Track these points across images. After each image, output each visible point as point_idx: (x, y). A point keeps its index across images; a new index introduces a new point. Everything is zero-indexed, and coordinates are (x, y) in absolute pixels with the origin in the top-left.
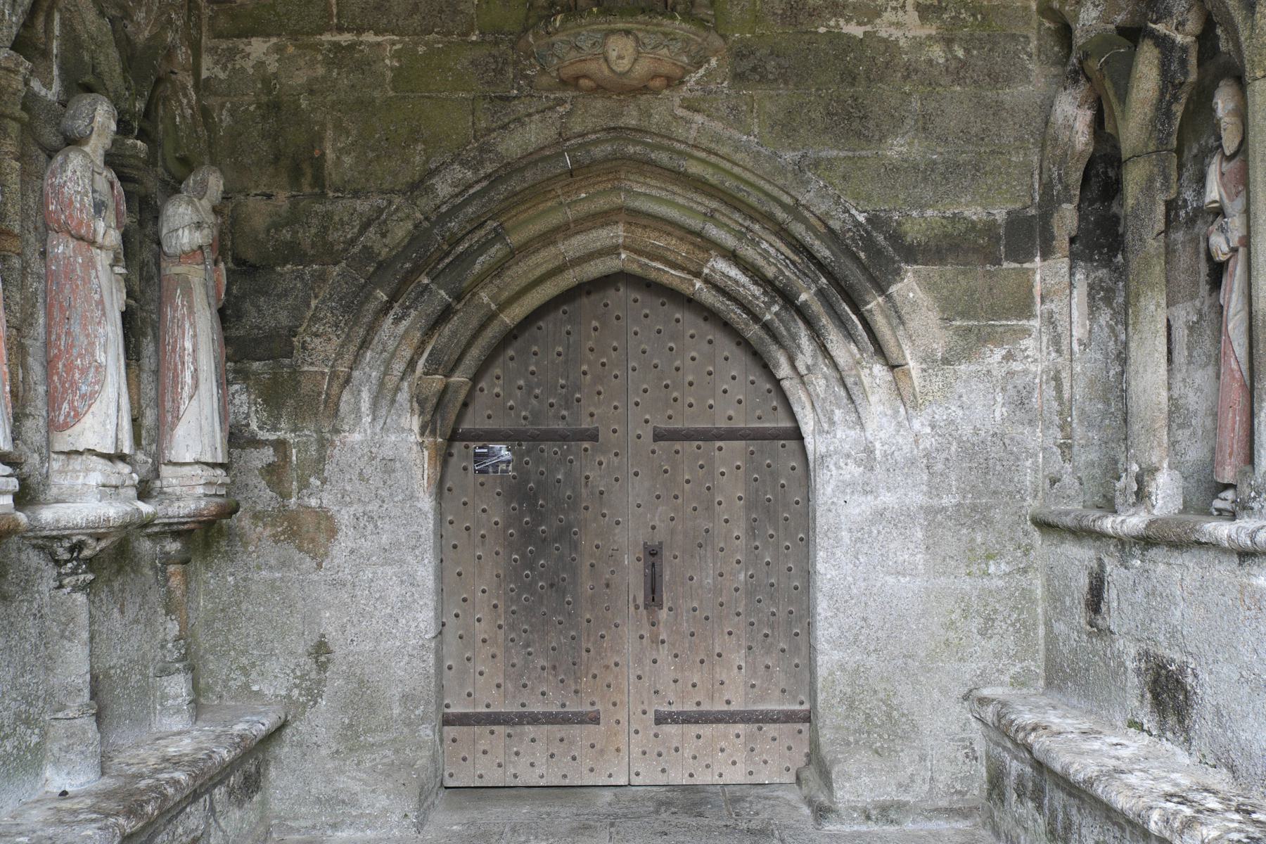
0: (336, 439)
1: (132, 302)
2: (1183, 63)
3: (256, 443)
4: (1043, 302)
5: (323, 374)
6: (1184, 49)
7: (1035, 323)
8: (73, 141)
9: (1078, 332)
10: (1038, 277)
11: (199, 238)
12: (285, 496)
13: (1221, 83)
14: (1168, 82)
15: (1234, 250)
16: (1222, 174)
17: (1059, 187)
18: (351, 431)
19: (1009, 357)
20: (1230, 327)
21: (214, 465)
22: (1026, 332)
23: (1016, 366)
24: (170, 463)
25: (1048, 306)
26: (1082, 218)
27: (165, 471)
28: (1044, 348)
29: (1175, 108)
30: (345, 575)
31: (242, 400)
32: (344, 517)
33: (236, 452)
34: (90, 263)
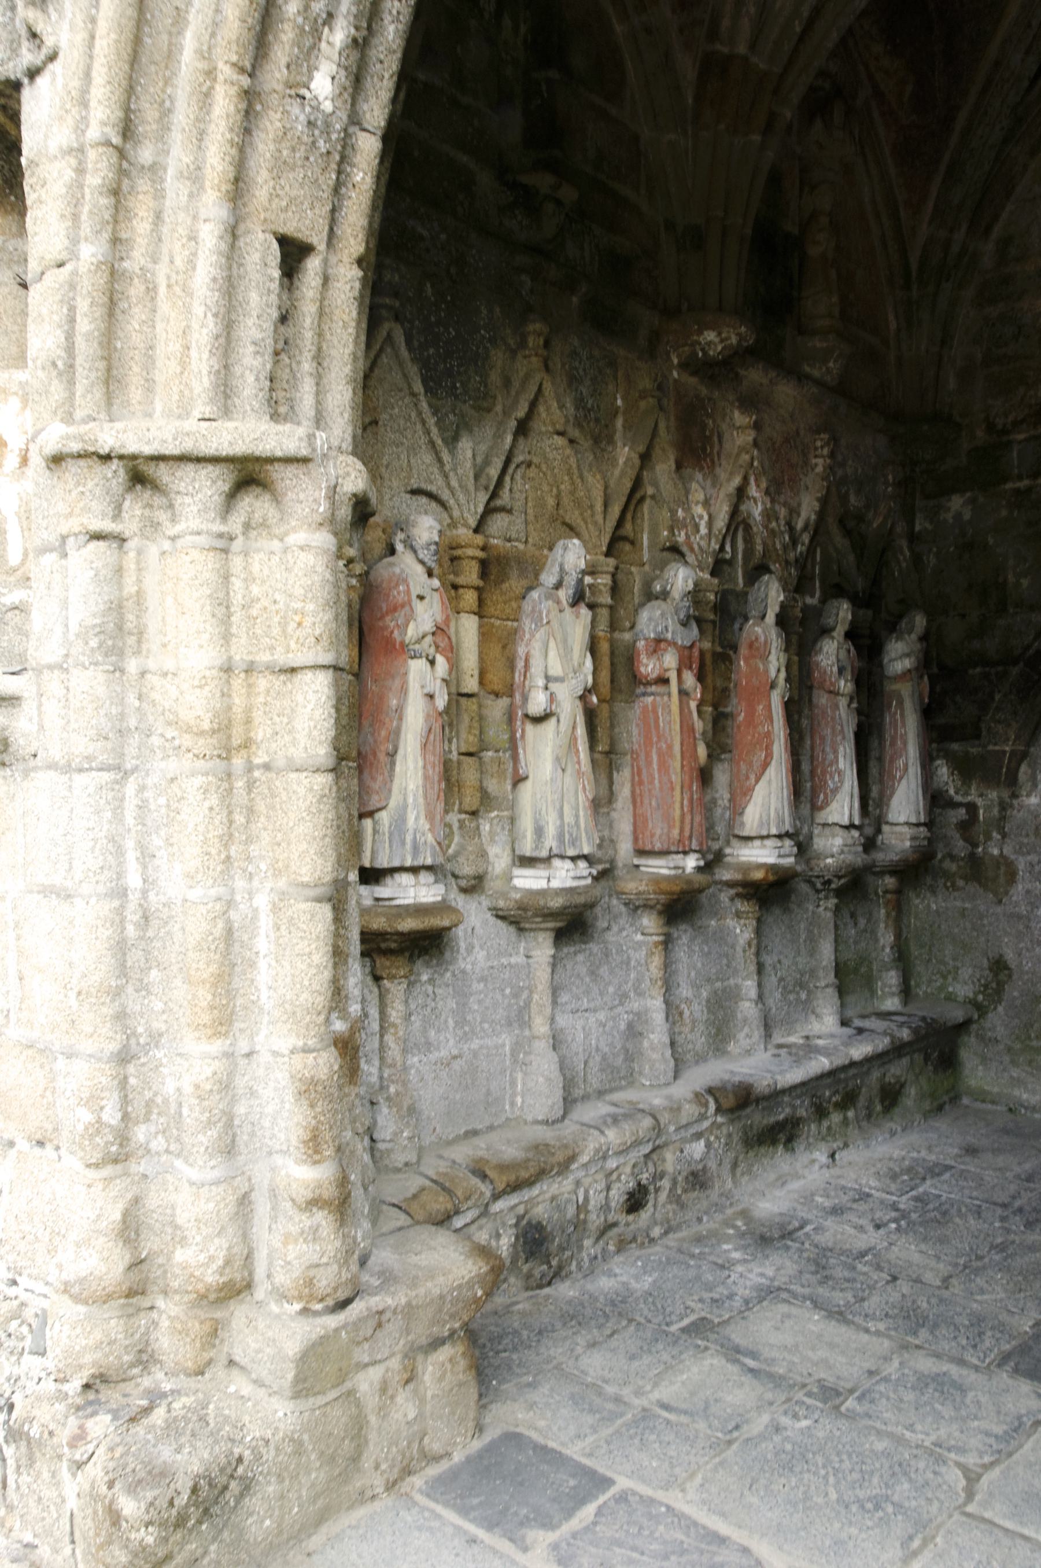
0: (1015, 802)
1: (863, 718)
3: (954, 805)
5: (1004, 752)
8: (826, 631)
11: (907, 664)
12: (975, 845)
18: (1028, 795)
21: (918, 825)
24: (887, 823)
27: (886, 828)
30: (1023, 909)
31: (943, 771)
32: (1021, 863)
33: (938, 811)
34: (836, 707)
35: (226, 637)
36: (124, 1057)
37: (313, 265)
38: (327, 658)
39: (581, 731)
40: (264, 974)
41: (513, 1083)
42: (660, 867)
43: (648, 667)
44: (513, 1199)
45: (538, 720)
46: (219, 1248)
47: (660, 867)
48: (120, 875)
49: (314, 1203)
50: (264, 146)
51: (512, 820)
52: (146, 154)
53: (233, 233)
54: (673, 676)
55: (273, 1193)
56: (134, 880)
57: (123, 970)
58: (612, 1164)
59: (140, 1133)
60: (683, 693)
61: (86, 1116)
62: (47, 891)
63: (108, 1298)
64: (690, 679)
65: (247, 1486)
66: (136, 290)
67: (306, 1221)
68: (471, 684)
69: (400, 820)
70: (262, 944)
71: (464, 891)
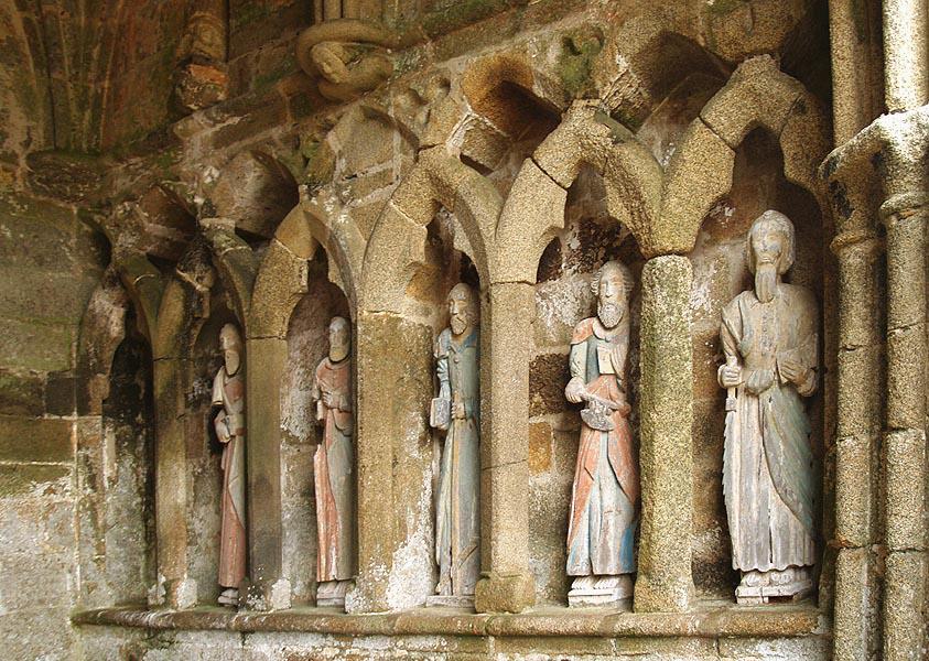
2: (200, 304)
4: (79, 448)
6: (201, 295)
7: (71, 465)
9: (107, 472)
10: (75, 428)
13: (226, 326)
14: (188, 313)
15: (233, 437)
16: (225, 385)
17: (95, 360)
19: (50, 491)
20: (230, 486)
22: (65, 472)
23: (56, 499)
25: (82, 452)
26: (113, 385)
28: (80, 485)
29: (193, 331)
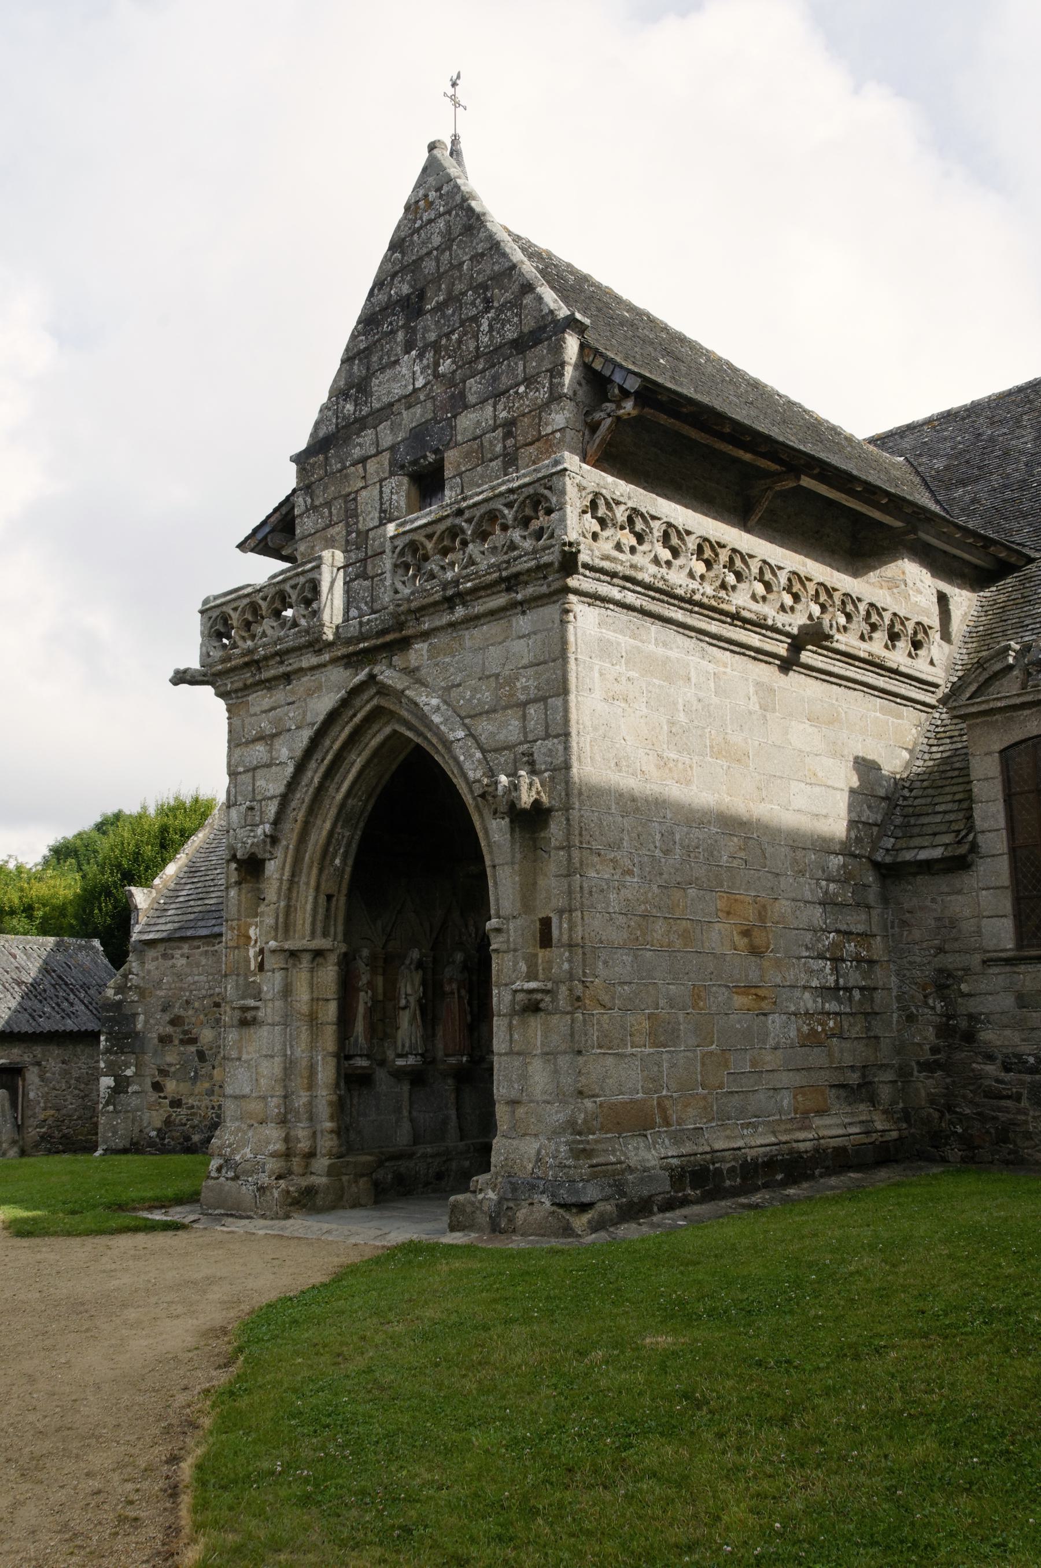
35: (312, 992)
36: (285, 1097)
37: (335, 899)
38: (336, 997)
39: (418, 1012)
40: (320, 1076)
41: (396, 1133)
42: (452, 1060)
43: (447, 988)
44: (392, 1163)
45: (404, 1008)
46: (308, 1143)
47: (452, 1060)
48: (286, 1051)
49: (332, 1132)
50: (324, 877)
51: (395, 1042)
52: (296, 880)
53: (316, 898)
54: (456, 991)
55: (322, 1132)
56: (289, 1053)
57: (286, 1075)
58: (430, 1160)
59: (289, 1117)
60: (460, 997)
61: (277, 1111)
62: (266, 1056)
63: (282, 1156)
64: (463, 992)
65: (317, 1193)
66: (292, 909)
67: (330, 1136)
68: (380, 998)
69: (356, 1040)
70: (320, 1069)
71: (378, 1065)
